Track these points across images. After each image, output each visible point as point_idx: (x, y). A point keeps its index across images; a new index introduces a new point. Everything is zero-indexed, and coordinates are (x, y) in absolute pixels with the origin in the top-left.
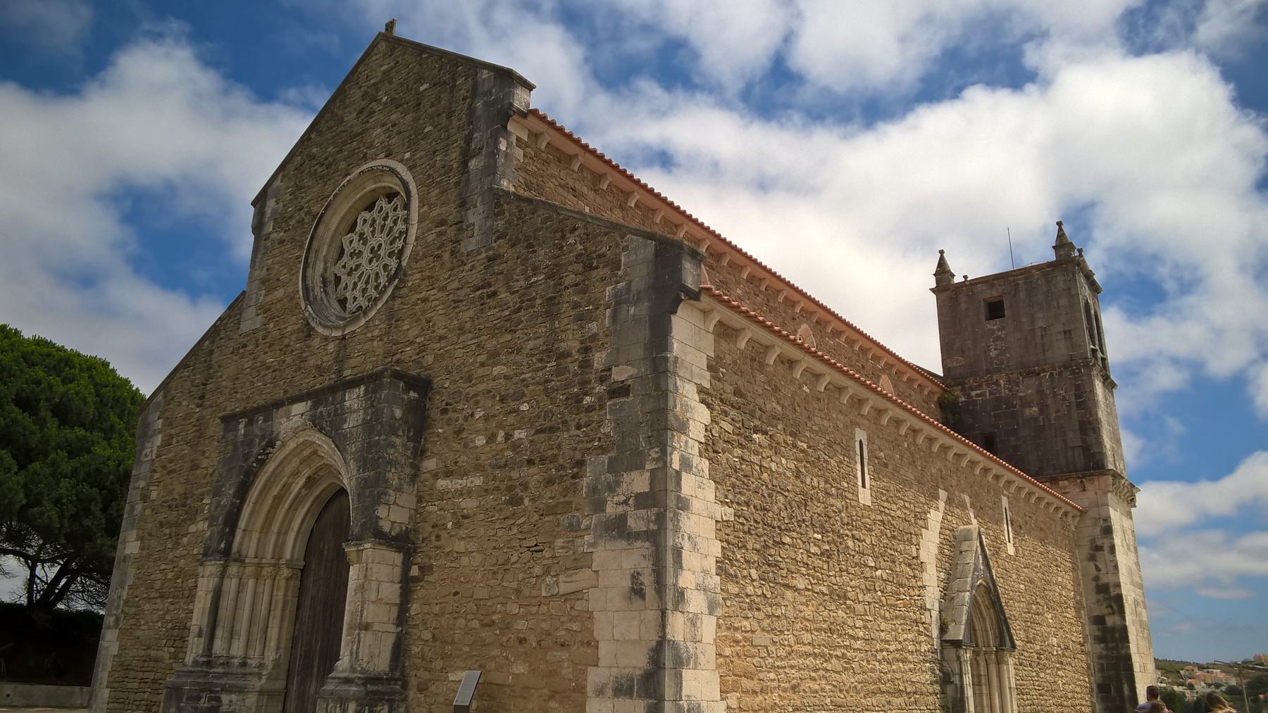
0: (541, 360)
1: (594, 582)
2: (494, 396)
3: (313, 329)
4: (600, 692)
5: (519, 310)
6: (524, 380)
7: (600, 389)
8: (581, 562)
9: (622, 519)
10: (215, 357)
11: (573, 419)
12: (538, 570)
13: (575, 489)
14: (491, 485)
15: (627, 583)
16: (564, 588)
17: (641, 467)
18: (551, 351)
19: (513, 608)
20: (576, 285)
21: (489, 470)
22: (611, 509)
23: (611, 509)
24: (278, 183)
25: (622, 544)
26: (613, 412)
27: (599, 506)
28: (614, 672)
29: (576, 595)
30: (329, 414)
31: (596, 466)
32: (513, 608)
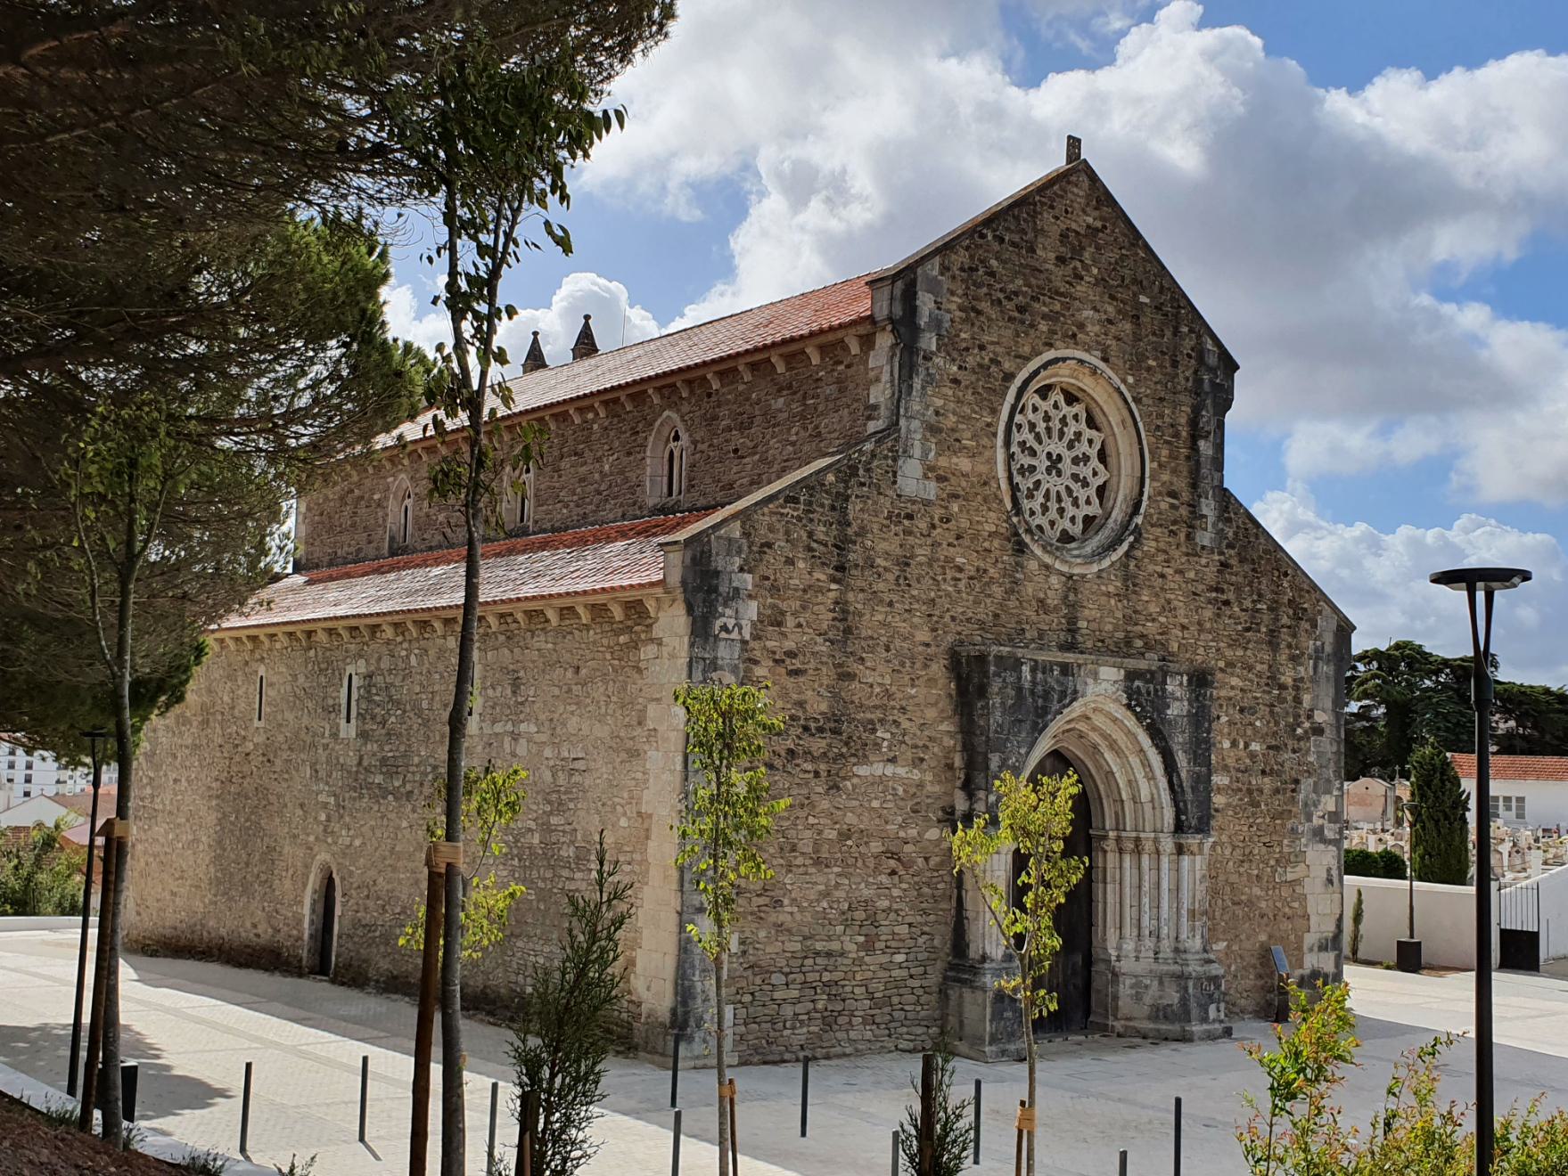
0: (1267, 685)
1: (1306, 873)
2: (1234, 706)
3: (1026, 545)
4: (1311, 950)
5: (1248, 629)
6: (1256, 698)
7: (1307, 725)
8: (1300, 857)
9: (1321, 828)
10: (854, 508)
11: (1290, 743)
12: (1272, 862)
13: (1293, 800)
14: (1235, 786)
15: (1325, 876)
16: (1290, 877)
17: (1329, 792)
18: (1273, 680)
19: (1257, 891)
20: (1289, 627)
21: (1233, 772)
22: (1316, 821)
23: (1316, 821)
24: (933, 268)
25: (1322, 846)
26: (1315, 746)
27: (1309, 818)
28: (1318, 936)
29: (1297, 882)
30: (1149, 693)
31: (1306, 785)
32: (1257, 891)
